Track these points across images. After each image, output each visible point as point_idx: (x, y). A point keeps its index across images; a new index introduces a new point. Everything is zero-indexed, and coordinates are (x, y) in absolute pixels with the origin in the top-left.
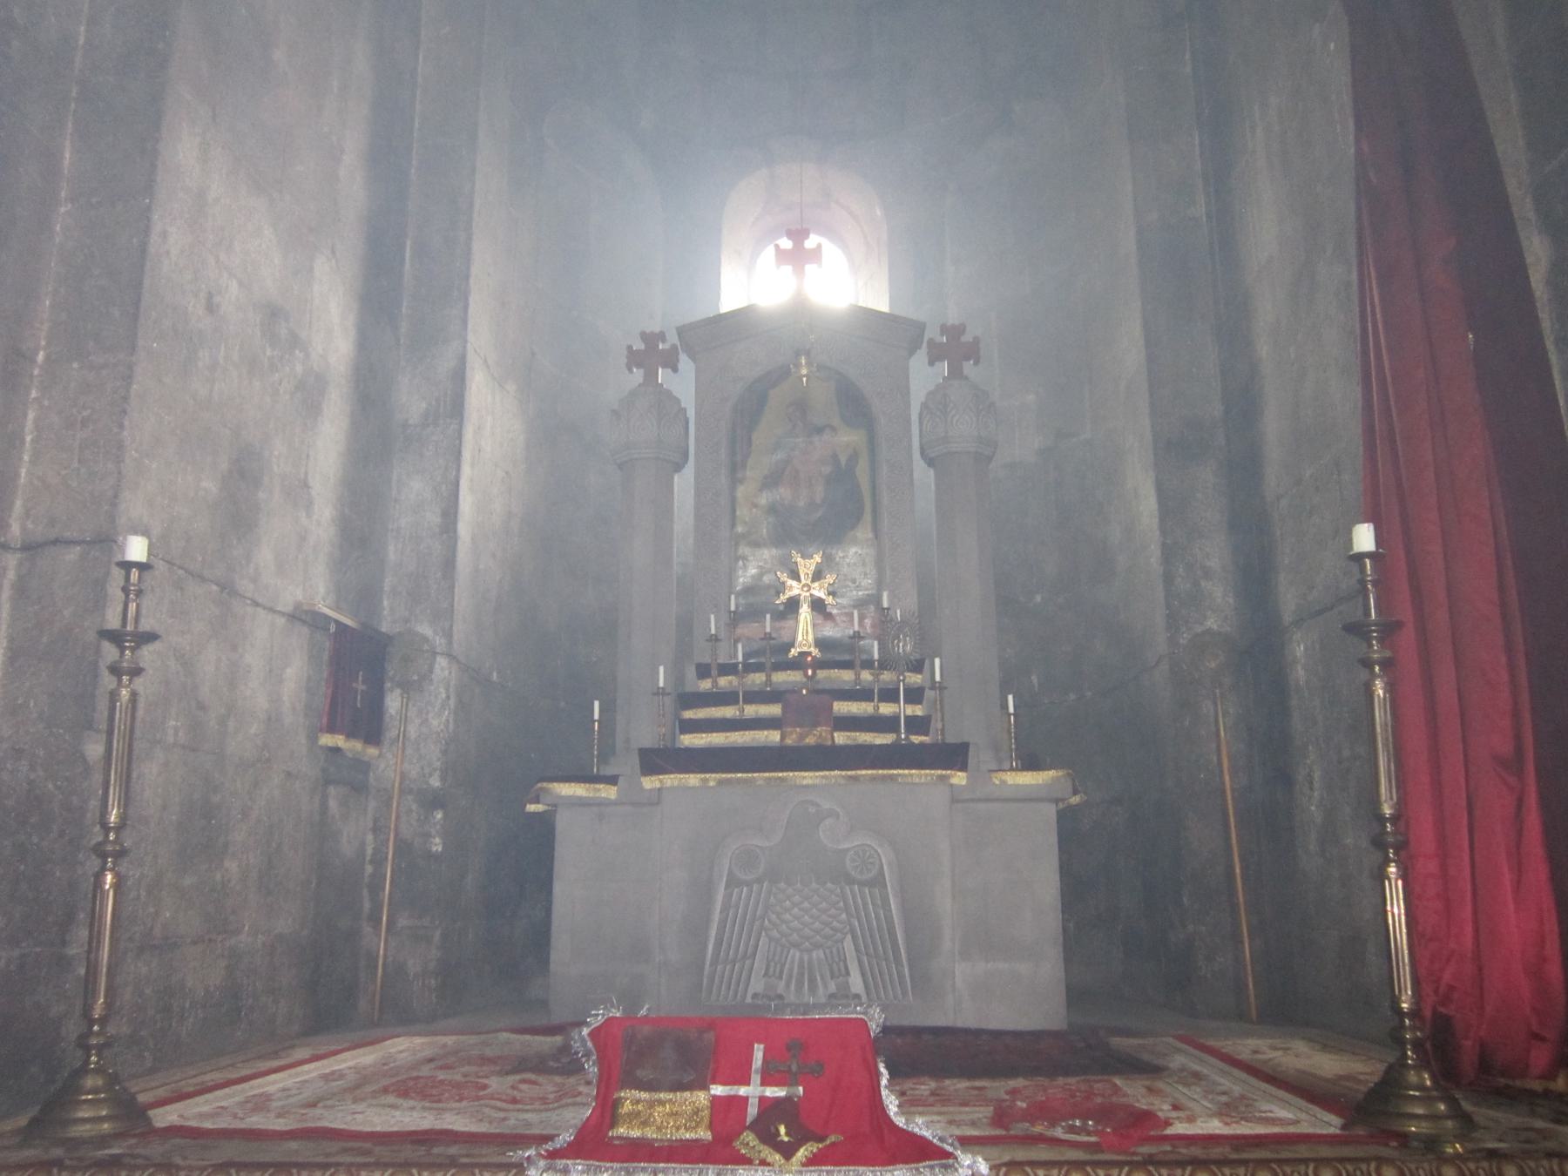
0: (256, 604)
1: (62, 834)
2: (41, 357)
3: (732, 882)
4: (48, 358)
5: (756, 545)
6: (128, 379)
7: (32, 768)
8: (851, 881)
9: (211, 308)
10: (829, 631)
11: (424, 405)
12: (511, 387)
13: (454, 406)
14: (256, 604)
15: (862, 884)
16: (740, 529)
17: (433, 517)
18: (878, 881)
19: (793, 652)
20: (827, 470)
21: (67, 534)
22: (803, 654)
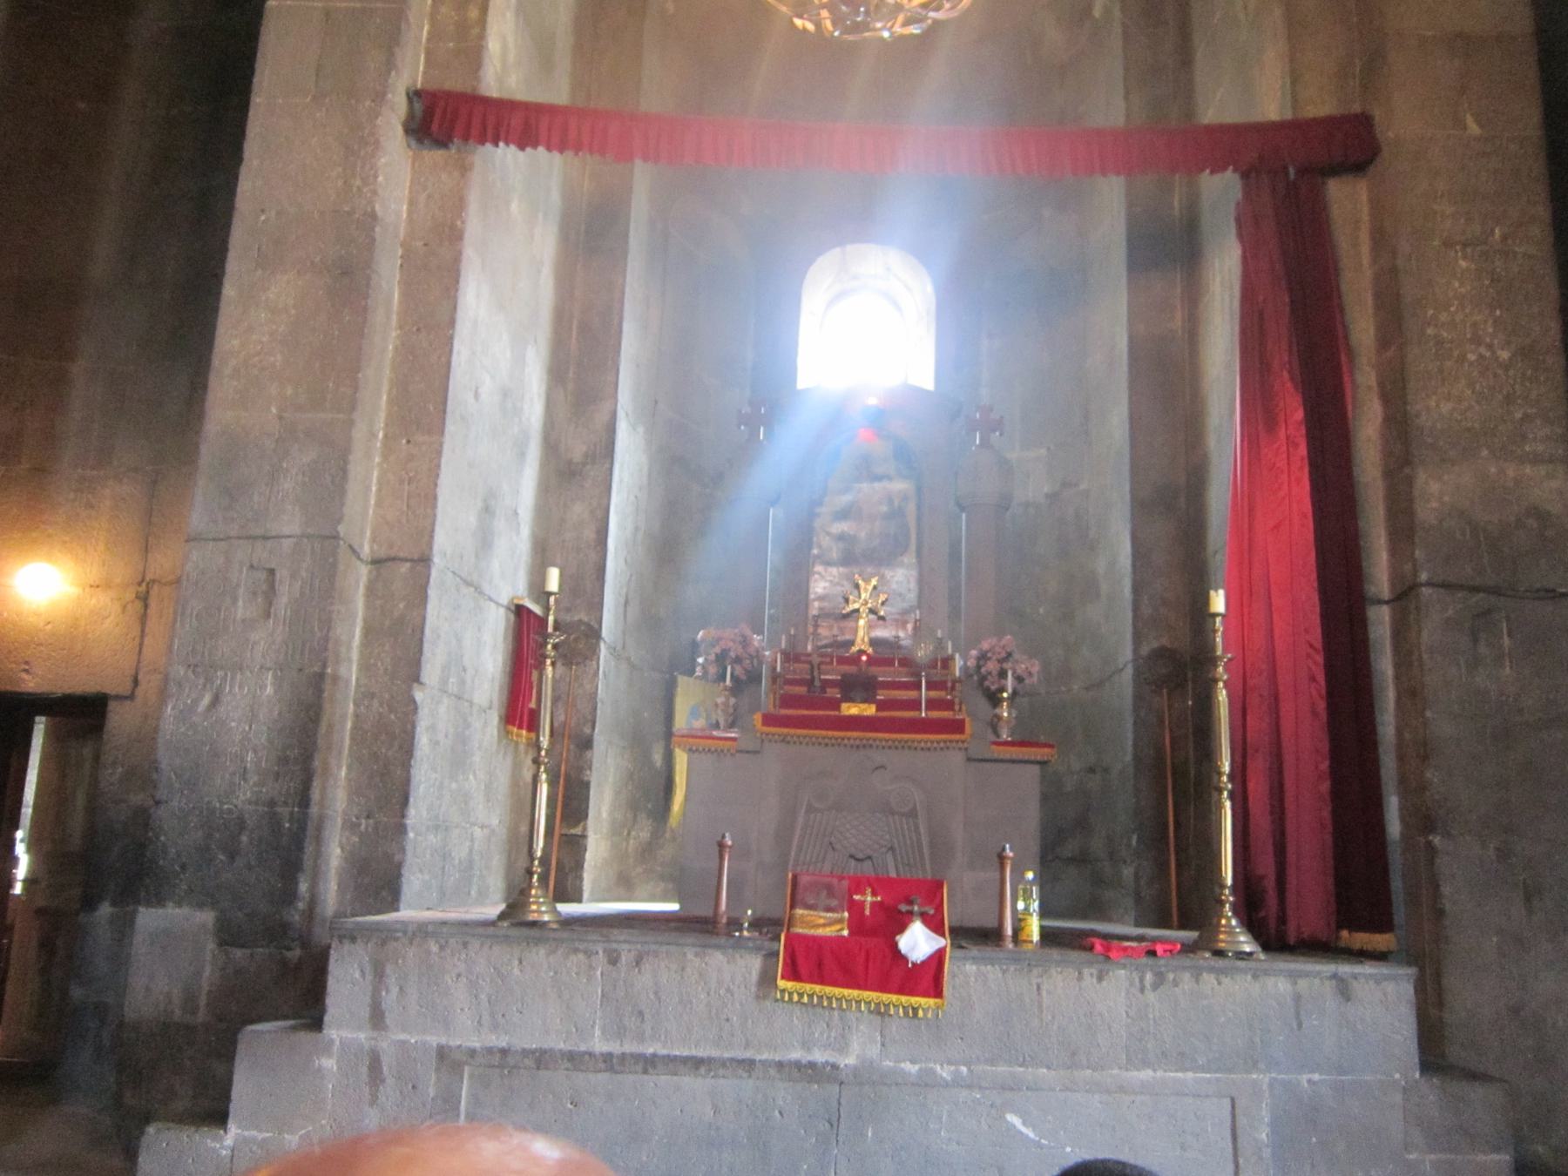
0: (490, 599)
1: (401, 747)
2: (381, 435)
3: (810, 809)
4: (386, 436)
5: (828, 563)
6: (439, 453)
7: (381, 705)
8: (893, 813)
9: (477, 395)
10: (882, 633)
11: (584, 448)
12: (641, 429)
13: (606, 450)
14: (490, 599)
15: (903, 815)
16: (815, 551)
17: (589, 534)
18: (913, 814)
19: (854, 649)
20: (884, 508)
21: (402, 555)
22: (861, 652)
